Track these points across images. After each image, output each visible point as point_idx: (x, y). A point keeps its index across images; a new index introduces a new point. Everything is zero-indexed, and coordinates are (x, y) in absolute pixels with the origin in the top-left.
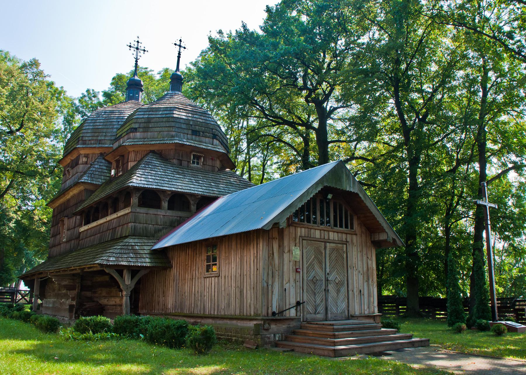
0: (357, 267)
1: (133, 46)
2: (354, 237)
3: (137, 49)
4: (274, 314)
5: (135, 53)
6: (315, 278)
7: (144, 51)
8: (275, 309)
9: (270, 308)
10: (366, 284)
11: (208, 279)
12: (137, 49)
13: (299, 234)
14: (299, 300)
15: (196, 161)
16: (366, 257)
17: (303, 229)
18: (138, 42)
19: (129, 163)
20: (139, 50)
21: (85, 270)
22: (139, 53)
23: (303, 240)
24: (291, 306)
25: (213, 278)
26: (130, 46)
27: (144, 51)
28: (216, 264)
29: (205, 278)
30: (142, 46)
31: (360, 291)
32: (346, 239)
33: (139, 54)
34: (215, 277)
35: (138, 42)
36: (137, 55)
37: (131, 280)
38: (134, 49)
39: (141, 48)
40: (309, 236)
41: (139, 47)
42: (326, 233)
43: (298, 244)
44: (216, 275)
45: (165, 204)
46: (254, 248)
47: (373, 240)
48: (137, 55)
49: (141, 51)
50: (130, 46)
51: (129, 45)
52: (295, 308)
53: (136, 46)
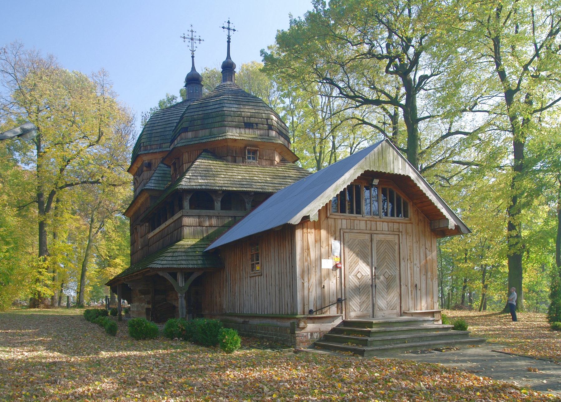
0: (412, 259)
1: (187, 36)
2: (409, 226)
3: (192, 39)
4: (311, 312)
5: (190, 44)
6: (359, 273)
7: (200, 40)
8: (312, 307)
9: (306, 306)
10: (423, 278)
12: (192, 39)
13: (339, 227)
14: (340, 297)
15: (251, 156)
16: (424, 249)
17: (344, 222)
18: (192, 31)
19: (184, 165)
22: (194, 44)
23: (344, 232)
24: (331, 304)
26: (184, 38)
27: (200, 40)
28: (258, 263)
29: (251, 277)
30: (196, 35)
31: (416, 286)
32: (399, 229)
33: (195, 45)
35: (192, 31)
36: (192, 47)
39: (196, 38)
40: (352, 228)
41: (194, 37)
42: (373, 223)
43: (338, 238)
44: (259, 274)
45: (218, 205)
46: (289, 244)
47: (433, 228)
48: (192, 47)
49: (196, 41)
50: (184, 38)
52: (336, 305)
53: (190, 37)
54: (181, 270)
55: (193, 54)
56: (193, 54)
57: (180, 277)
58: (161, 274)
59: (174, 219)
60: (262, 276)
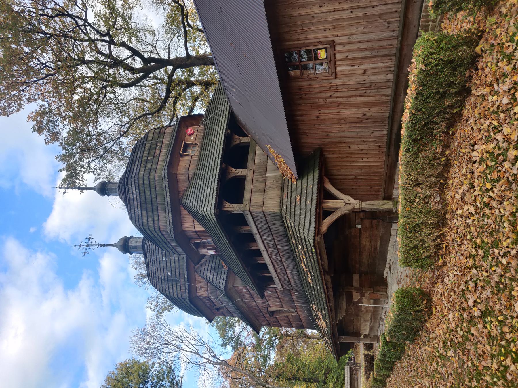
1: (84, 250)
3: (88, 245)
5: (92, 248)
7: (90, 238)
11: (338, 69)
12: (88, 245)
18: (80, 245)
20: (90, 243)
21: (326, 268)
22: (92, 244)
25: (338, 56)
26: (85, 253)
27: (90, 238)
34: (335, 50)
35: (80, 245)
36: (95, 245)
37: (339, 199)
38: (88, 249)
48: (95, 245)
49: (90, 242)
50: (85, 253)
51: (83, 254)
53: (85, 247)
54: (319, 204)
55: (101, 245)
56: (101, 245)
57: (330, 204)
58: (324, 228)
59: (257, 232)
60: (336, 39)
